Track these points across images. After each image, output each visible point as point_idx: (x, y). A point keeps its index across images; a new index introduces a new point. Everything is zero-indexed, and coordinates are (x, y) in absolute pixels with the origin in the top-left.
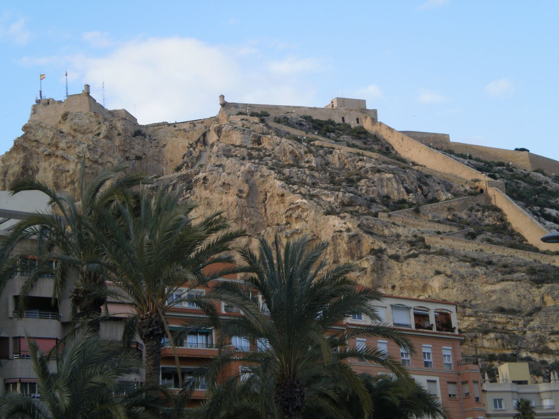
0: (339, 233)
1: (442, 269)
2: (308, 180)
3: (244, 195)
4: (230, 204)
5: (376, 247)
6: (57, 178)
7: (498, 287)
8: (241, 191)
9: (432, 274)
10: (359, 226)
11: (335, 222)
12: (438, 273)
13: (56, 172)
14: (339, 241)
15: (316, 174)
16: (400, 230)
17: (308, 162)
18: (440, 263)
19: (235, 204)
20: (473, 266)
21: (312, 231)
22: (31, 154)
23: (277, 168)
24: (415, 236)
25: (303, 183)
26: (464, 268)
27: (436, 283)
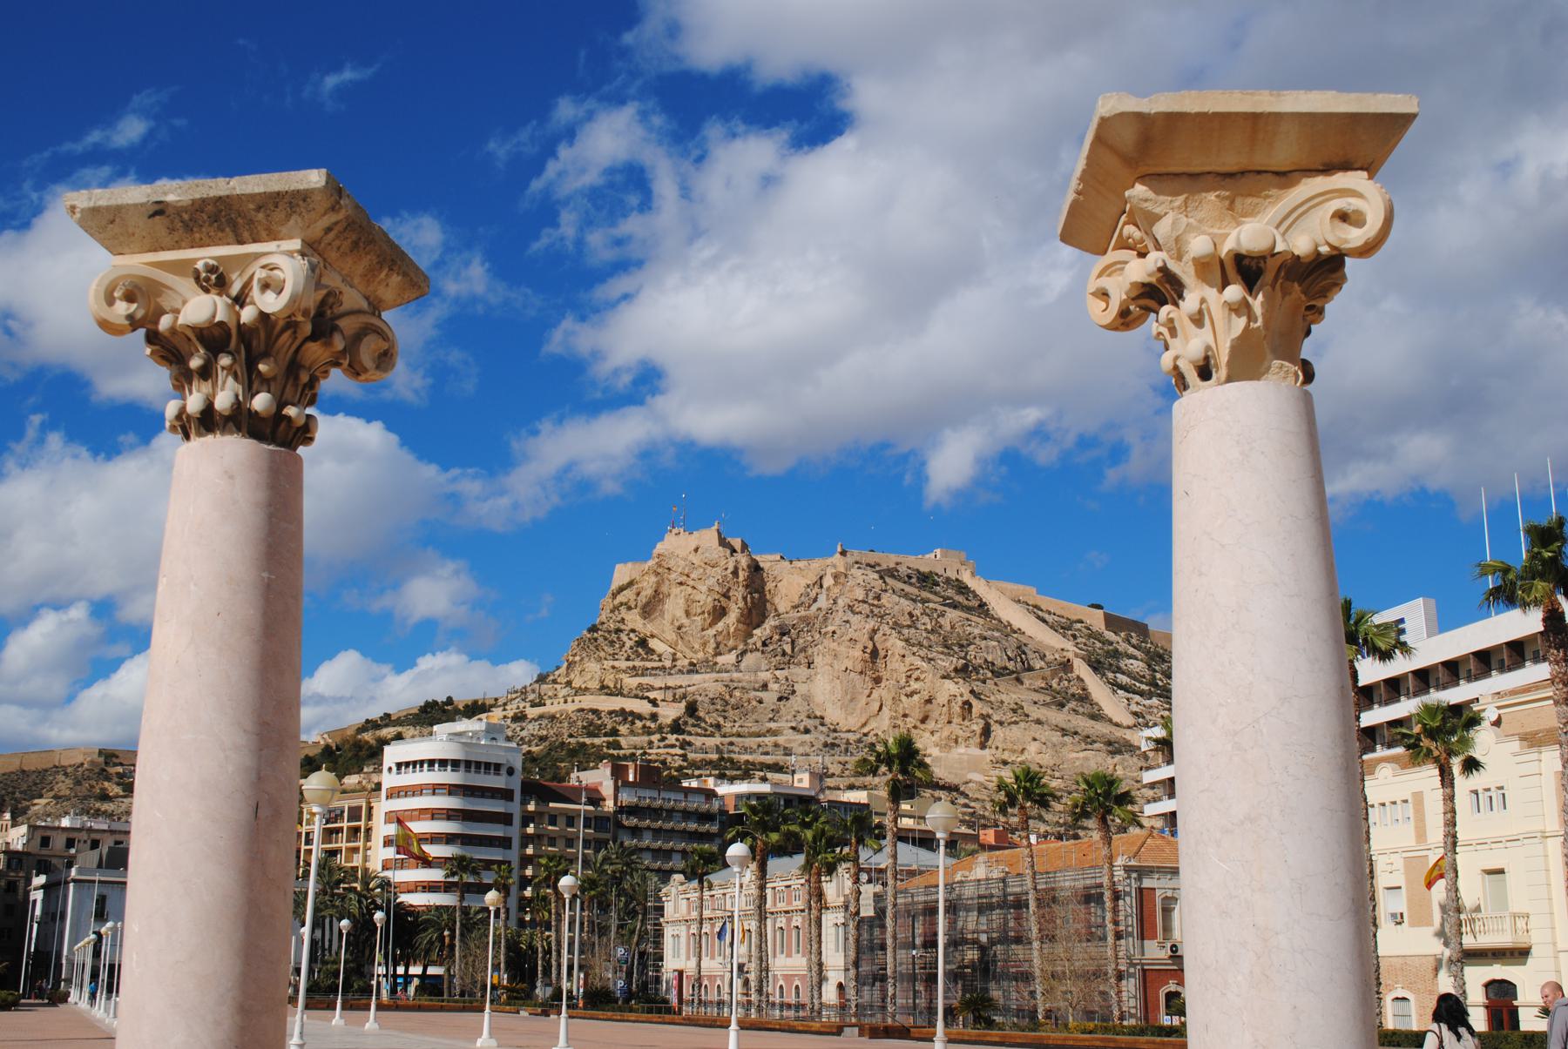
1: (1037, 737)
2: (925, 643)
5: (984, 713)
7: (1082, 755)
9: (1030, 739)
11: (948, 684)
12: (1035, 739)
15: (932, 637)
16: (1004, 697)
18: (1036, 730)
20: (1063, 736)
23: (896, 626)
25: (920, 645)
26: (1056, 737)
27: (1033, 748)
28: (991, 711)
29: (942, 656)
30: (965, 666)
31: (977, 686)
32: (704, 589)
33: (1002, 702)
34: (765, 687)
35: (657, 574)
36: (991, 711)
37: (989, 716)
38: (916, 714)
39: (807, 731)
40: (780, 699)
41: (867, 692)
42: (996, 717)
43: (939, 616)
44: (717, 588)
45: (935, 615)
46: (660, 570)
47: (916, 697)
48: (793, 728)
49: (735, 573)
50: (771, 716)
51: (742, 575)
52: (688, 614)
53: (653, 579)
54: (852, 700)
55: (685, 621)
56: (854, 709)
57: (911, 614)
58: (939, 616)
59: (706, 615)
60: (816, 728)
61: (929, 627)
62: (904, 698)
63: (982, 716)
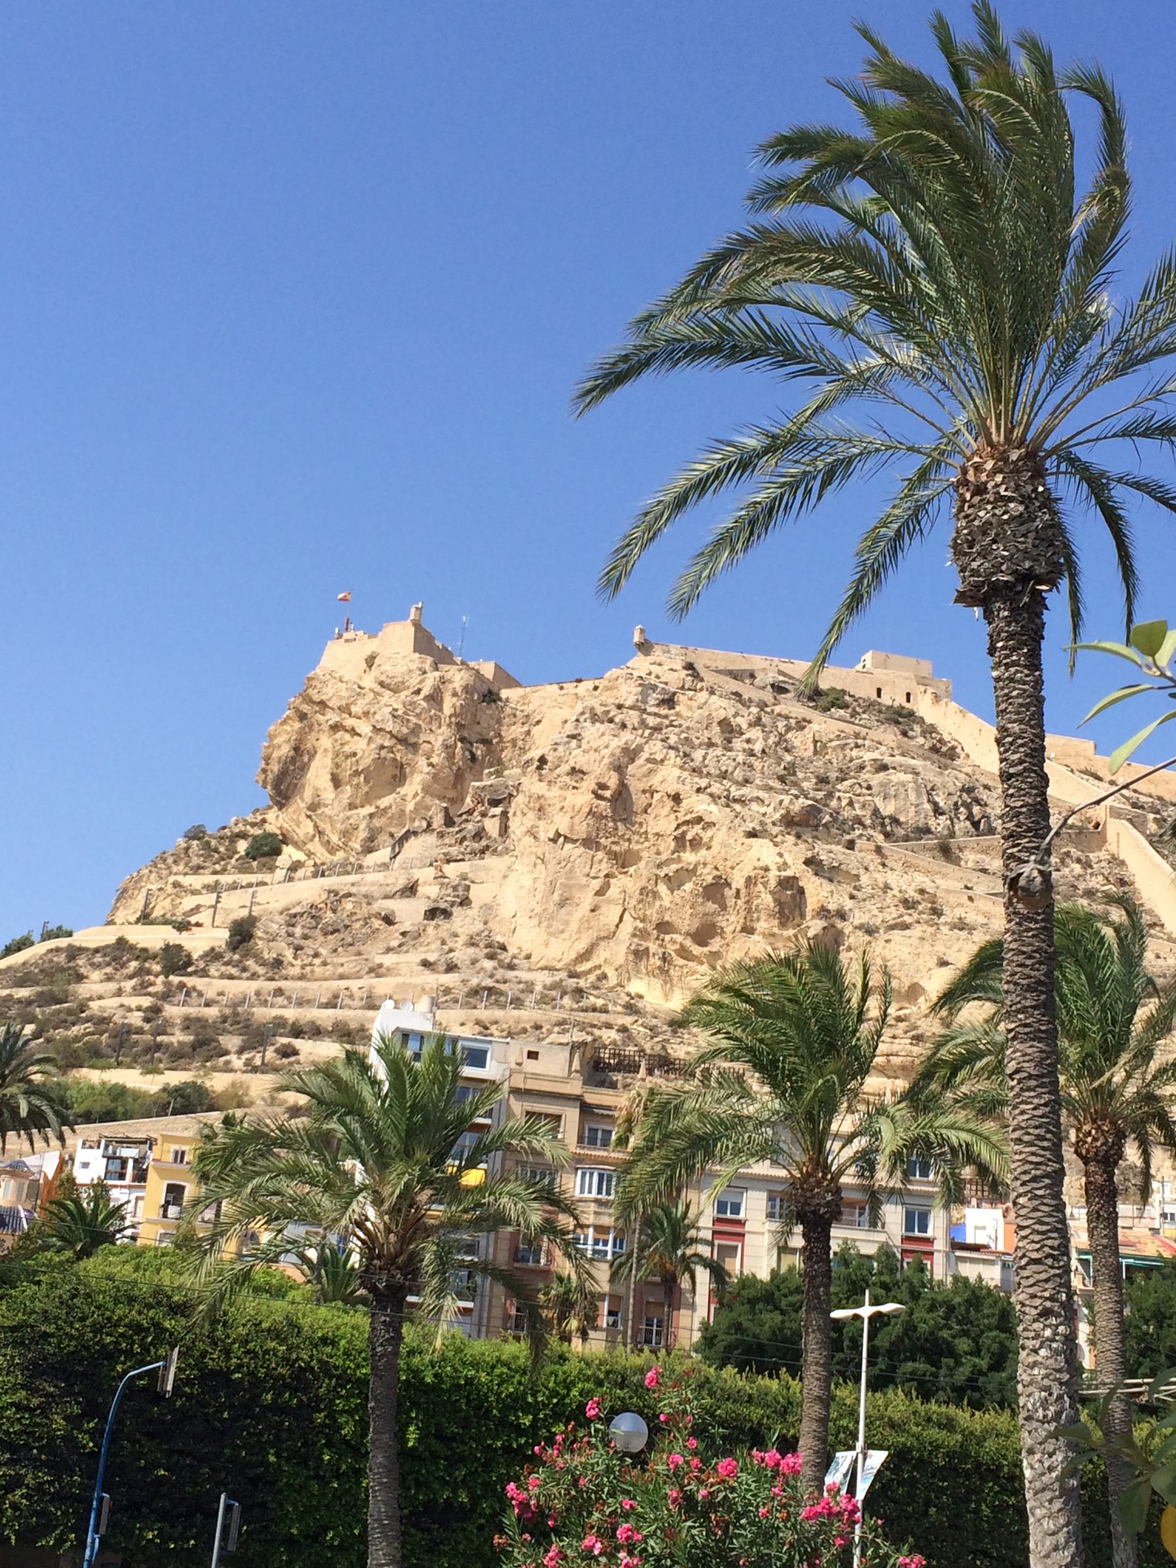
0: (762, 872)
3: (608, 794)
4: (577, 809)
5: (832, 907)
6: (337, 766)
8: (603, 786)
10: (808, 862)
11: (763, 852)
13: (337, 756)
14: (760, 887)
16: (893, 878)
17: (748, 741)
19: (587, 810)
21: (716, 868)
22: (311, 727)
24: (922, 891)
28: (848, 904)
29: (761, 794)
30: (813, 812)
31: (829, 852)
32: (364, 728)
33: (887, 887)
34: (411, 890)
35: (302, 717)
36: (848, 904)
37: (842, 915)
38: (685, 920)
39: (451, 968)
40: (432, 914)
41: (596, 884)
42: (858, 918)
43: (789, 729)
44: (390, 726)
45: (781, 725)
46: (305, 708)
47: (688, 886)
48: (426, 964)
49: (435, 698)
50: (395, 943)
51: (449, 704)
52: (336, 782)
53: (297, 725)
54: (562, 904)
55: (328, 794)
56: (567, 923)
57: (725, 724)
58: (789, 729)
59: (362, 778)
60: (474, 962)
61: (758, 747)
62: (662, 889)
63: (823, 912)
